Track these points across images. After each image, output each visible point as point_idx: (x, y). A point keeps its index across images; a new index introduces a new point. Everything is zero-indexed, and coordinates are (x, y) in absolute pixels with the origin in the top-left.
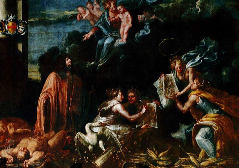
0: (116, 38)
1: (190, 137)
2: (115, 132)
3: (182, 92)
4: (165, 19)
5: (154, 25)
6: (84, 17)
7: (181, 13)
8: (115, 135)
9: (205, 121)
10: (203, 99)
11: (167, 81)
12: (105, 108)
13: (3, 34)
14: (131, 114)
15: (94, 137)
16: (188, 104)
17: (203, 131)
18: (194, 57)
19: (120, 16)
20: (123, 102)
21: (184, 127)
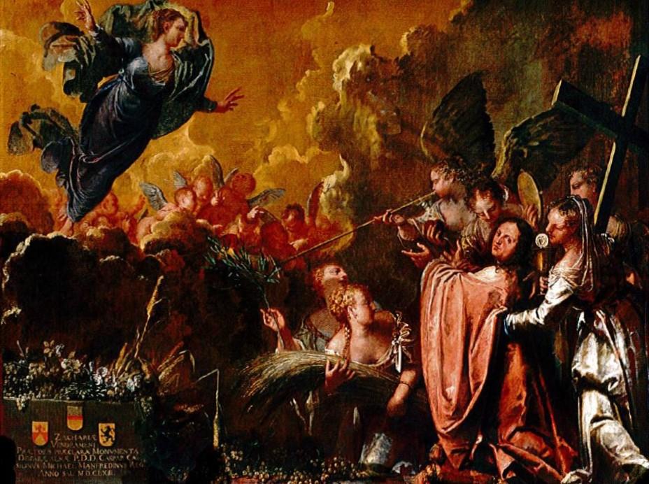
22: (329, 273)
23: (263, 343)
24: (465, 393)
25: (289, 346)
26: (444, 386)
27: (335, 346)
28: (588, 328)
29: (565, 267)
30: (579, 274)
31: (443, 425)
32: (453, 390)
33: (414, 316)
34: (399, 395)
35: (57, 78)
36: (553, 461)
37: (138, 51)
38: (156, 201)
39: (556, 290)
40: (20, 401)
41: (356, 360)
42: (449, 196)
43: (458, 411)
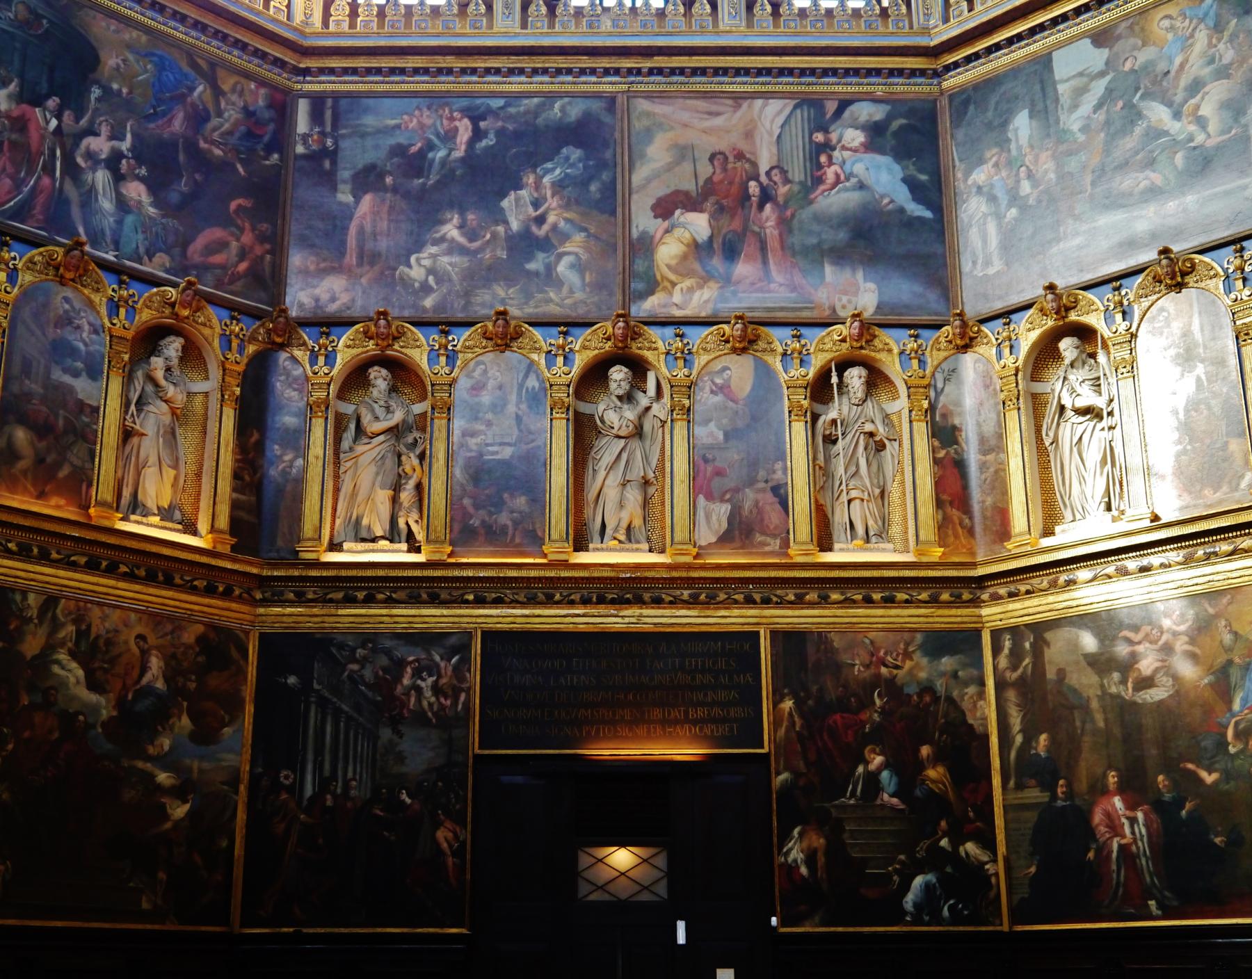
0: (451, 150)
1: (550, 269)
2: (450, 264)
3: (538, 213)
4: (515, 125)
5: (500, 133)
6: (411, 126)
7: (536, 118)
8: (450, 268)
9: (568, 247)
10: (567, 220)
11: (517, 200)
12: (437, 235)
13: (306, 148)
14: (471, 240)
15: (423, 271)
16: (546, 227)
17: (566, 261)
18: (553, 169)
19: (457, 123)
20: (461, 227)
21: (541, 256)
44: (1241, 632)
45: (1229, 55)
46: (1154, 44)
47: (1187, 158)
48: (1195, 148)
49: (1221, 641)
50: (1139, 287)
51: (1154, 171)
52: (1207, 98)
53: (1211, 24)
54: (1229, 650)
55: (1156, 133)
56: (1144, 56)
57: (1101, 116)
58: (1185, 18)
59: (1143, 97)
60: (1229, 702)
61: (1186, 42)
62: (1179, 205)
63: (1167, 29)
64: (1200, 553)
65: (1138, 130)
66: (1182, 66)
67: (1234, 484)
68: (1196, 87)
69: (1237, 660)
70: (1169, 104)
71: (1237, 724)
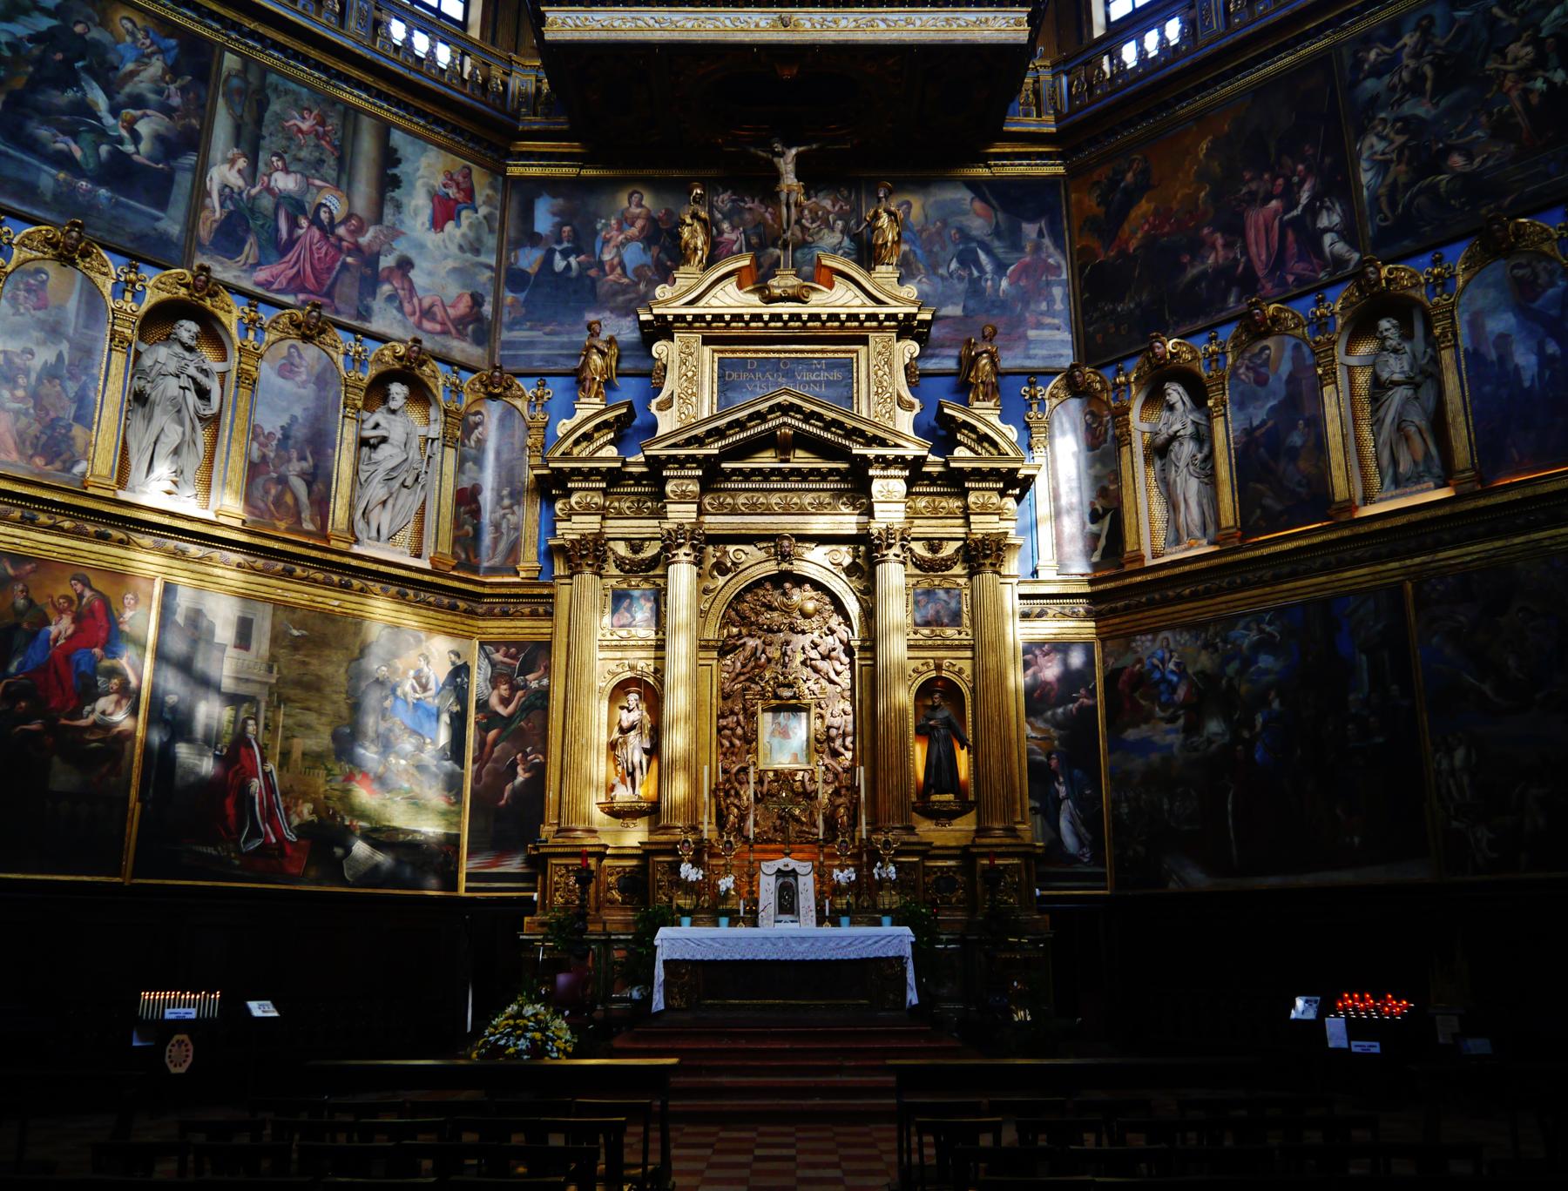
22: (1206, 231)
23: (1182, 268)
24: (1269, 256)
25: (1193, 266)
26: (1259, 255)
27: (1211, 261)
28: (1321, 207)
29: (1307, 186)
30: (1314, 187)
31: (1260, 274)
32: (1263, 257)
33: (1242, 234)
34: (1240, 268)
35: (1094, 203)
36: (1313, 271)
37: (1123, 179)
38: (1134, 233)
39: (1304, 198)
40: (1091, 329)
41: (1220, 261)
42: (1251, 180)
43: (1267, 265)
44: (37, 601)
45: (176, 101)
46: (112, 33)
47: (110, 153)
48: (121, 152)
49: (14, 604)
50: (28, 236)
51: (76, 142)
52: (146, 119)
53: (170, 62)
54: (20, 614)
55: (85, 109)
56: (95, 34)
57: (35, 50)
58: (147, 36)
59: (83, 68)
60: (7, 663)
61: (143, 59)
62: (89, 191)
63: (127, 30)
64: (17, 513)
65: (70, 94)
66: (133, 74)
67: (68, 465)
68: (138, 102)
69: (25, 626)
70: (109, 94)
71: (7, 685)
